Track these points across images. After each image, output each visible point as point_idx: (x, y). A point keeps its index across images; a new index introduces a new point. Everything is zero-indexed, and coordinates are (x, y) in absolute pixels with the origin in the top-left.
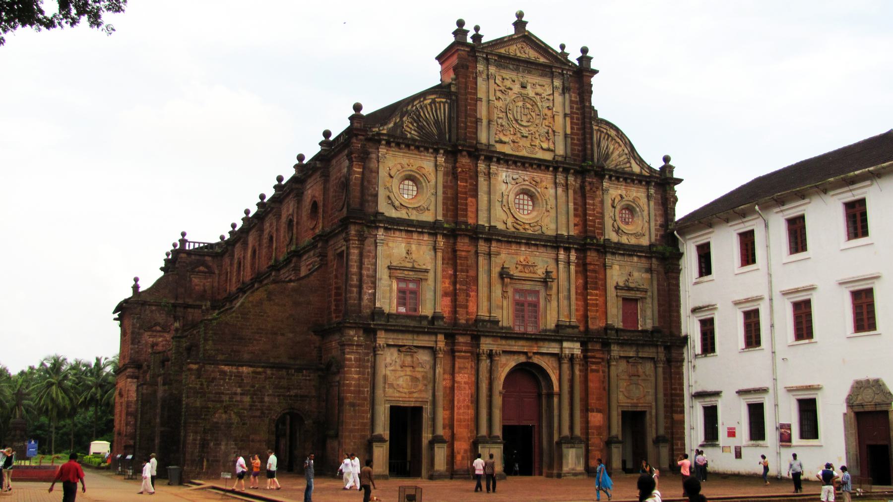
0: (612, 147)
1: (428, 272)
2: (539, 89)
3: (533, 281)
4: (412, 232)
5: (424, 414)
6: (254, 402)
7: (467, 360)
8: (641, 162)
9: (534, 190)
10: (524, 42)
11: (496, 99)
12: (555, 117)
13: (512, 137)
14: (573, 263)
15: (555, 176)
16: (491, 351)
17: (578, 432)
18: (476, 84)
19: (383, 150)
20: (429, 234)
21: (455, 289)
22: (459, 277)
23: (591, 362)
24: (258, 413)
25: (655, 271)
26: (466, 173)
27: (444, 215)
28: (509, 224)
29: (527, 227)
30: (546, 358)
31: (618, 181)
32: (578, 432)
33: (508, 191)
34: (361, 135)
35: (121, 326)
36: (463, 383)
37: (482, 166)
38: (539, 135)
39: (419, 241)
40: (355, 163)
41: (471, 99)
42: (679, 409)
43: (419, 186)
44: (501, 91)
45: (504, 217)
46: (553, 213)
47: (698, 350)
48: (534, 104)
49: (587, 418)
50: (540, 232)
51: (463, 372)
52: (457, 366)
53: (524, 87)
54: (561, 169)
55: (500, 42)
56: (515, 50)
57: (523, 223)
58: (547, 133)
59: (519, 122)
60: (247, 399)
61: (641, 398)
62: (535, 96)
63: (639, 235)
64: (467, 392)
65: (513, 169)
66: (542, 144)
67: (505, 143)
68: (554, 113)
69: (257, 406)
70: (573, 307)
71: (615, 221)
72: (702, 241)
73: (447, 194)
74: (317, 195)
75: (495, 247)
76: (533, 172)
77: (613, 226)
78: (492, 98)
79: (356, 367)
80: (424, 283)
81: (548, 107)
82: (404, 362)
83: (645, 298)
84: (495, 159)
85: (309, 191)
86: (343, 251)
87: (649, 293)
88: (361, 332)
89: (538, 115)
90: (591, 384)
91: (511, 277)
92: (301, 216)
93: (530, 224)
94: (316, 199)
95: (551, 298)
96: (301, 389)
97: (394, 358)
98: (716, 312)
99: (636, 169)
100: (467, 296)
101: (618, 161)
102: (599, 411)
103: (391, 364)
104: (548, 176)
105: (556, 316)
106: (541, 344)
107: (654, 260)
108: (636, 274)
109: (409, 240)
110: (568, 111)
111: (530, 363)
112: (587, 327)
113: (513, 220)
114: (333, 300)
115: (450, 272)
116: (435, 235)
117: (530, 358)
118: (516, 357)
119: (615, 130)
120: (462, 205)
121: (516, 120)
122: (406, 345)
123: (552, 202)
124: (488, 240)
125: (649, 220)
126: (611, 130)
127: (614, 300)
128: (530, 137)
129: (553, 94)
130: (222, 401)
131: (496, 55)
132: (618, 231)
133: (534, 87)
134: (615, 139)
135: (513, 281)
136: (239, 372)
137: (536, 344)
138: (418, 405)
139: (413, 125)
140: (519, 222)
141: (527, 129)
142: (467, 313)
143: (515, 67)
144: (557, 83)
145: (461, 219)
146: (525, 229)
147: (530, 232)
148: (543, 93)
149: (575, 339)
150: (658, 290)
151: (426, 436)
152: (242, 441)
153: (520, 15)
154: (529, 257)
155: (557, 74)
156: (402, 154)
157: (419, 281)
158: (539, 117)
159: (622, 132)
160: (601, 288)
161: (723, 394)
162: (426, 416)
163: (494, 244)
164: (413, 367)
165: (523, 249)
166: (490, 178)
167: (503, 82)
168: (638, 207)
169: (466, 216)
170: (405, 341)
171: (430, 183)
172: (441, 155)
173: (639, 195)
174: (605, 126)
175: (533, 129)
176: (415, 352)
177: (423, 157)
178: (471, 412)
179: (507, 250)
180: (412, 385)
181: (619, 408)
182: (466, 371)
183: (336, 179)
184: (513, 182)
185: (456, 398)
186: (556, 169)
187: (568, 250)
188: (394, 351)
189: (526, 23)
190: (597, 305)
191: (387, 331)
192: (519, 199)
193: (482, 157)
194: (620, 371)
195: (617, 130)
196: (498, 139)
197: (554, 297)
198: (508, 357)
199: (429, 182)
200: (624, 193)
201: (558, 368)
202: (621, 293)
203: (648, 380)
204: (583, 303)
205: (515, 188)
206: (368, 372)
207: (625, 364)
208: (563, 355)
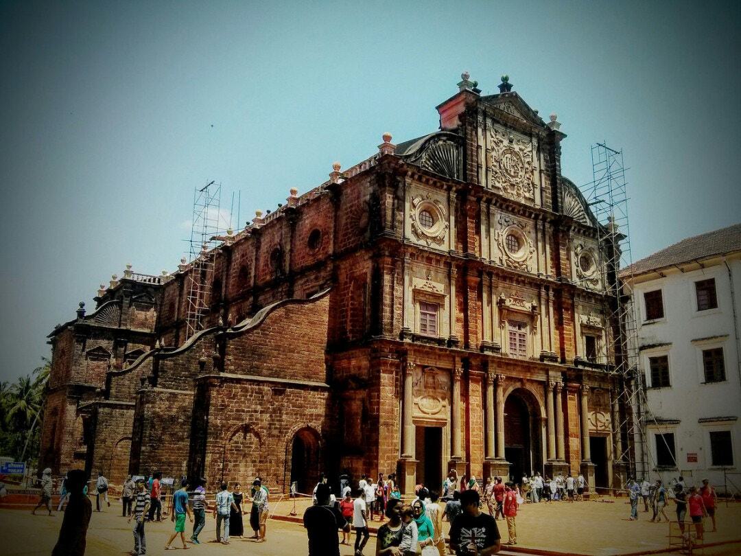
0: (573, 203)
6: (273, 420)
8: (593, 219)
9: (520, 233)
10: (510, 102)
12: (534, 171)
18: (477, 133)
19: (408, 180)
20: (446, 263)
21: (466, 316)
22: (470, 304)
32: (562, 455)
35: (54, 349)
37: (483, 206)
38: (523, 186)
40: (387, 188)
43: (435, 218)
44: (495, 142)
45: (501, 256)
47: (649, 382)
53: (511, 142)
54: (541, 217)
58: (529, 184)
60: (267, 416)
67: (499, 188)
70: (552, 340)
72: (652, 287)
74: (319, 223)
84: (494, 202)
85: (307, 222)
86: (366, 274)
91: (508, 309)
92: (295, 245)
93: (518, 263)
94: (318, 228)
96: (316, 408)
99: (589, 223)
101: (578, 215)
107: (606, 303)
110: (543, 168)
114: (348, 320)
121: (507, 170)
122: (429, 366)
124: (490, 274)
130: (243, 420)
132: (580, 277)
136: (259, 389)
137: (529, 371)
138: (438, 426)
139: (430, 162)
142: (477, 337)
144: (535, 141)
145: (470, 251)
151: (446, 458)
152: (260, 462)
153: (505, 79)
156: (422, 186)
164: (434, 388)
166: (489, 218)
167: (496, 135)
173: (593, 246)
178: (482, 435)
182: (477, 394)
183: (351, 206)
185: (471, 420)
186: (536, 218)
187: (547, 289)
188: (419, 371)
189: (511, 86)
192: (508, 239)
193: (484, 199)
195: (576, 189)
197: (539, 329)
200: (583, 244)
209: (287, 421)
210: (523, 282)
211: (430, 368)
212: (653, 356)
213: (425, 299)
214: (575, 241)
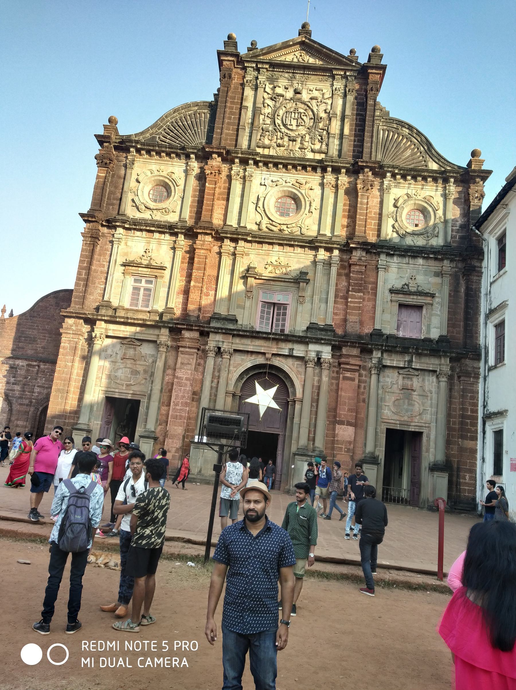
1: (165, 270)
2: (316, 94)
3: (284, 281)
4: (152, 232)
5: (140, 408)
7: (192, 357)
8: (439, 158)
12: (332, 119)
14: (335, 264)
17: (319, 443)
22: (194, 274)
24: (26, 402)
25: (446, 274)
26: (215, 175)
27: (191, 217)
29: (284, 227)
30: (290, 361)
33: (266, 192)
34: (106, 142)
36: (184, 379)
37: (236, 168)
44: (271, 99)
46: (316, 214)
49: (334, 429)
50: (299, 233)
51: (185, 368)
52: (179, 360)
53: (297, 92)
54: (329, 169)
55: (271, 50)
56: (293, 59)
57: (280, 224)
59: (289, 127)
61: (416, 416)
64: (188, 389)
66: (313, 146)
68: (331, 115)
69: (26, 395)
71: (396, 221)
76: (298, 174)
77: (393, 227)
78: (259, 105)
81: (325, 110)
82: (125, 354)
83: (432, 305)
84: (251, 162)
87: (437, 300)
89: (312, 119)
90: (342, 393)
95: (304, 300)
99: (434, 166)
102: (349, 424)
103: (111, 356)
105: (309, 319)
106: (283, 345)
109: (148, 239)
112: (345, 332)
116: (176, 234)
119: (408, 129)
120: (208, 205)
124: (235, 240)
126: (404, 129)
128: (299, 140)
129: (332, 97)
131: (266, 63)
133: (310, 92)
136: (14, 364)
137: (277, 344)
140: (274, 223)
143: (291, 75)
146: (280, 230)
147: (286, 232)
149: (323, 342)
155: (340, 77)
159: (417, 130)
161: (509, 413)
162: (142, 409)
163: (241, 243)
168: (431, 206)
172: (194, 160)
173: (432, 194)
174: (395, 126)
176: (140, 346)
180: (131, 378)
181: (383, 424)
182: (189, 367)
185: (174, 394)
186: (324, 170)
187: (329, 250)
190: (359, 307)
191: (106, 322)
195: (410, 128)
198: (242, 357)
199: (177, 186)
201: (303, 373)
202: (395, 297)
203: (427, 396)
204: (345, 307)
208: (307, 358)
209: (39, 393)
212: (496, 322)
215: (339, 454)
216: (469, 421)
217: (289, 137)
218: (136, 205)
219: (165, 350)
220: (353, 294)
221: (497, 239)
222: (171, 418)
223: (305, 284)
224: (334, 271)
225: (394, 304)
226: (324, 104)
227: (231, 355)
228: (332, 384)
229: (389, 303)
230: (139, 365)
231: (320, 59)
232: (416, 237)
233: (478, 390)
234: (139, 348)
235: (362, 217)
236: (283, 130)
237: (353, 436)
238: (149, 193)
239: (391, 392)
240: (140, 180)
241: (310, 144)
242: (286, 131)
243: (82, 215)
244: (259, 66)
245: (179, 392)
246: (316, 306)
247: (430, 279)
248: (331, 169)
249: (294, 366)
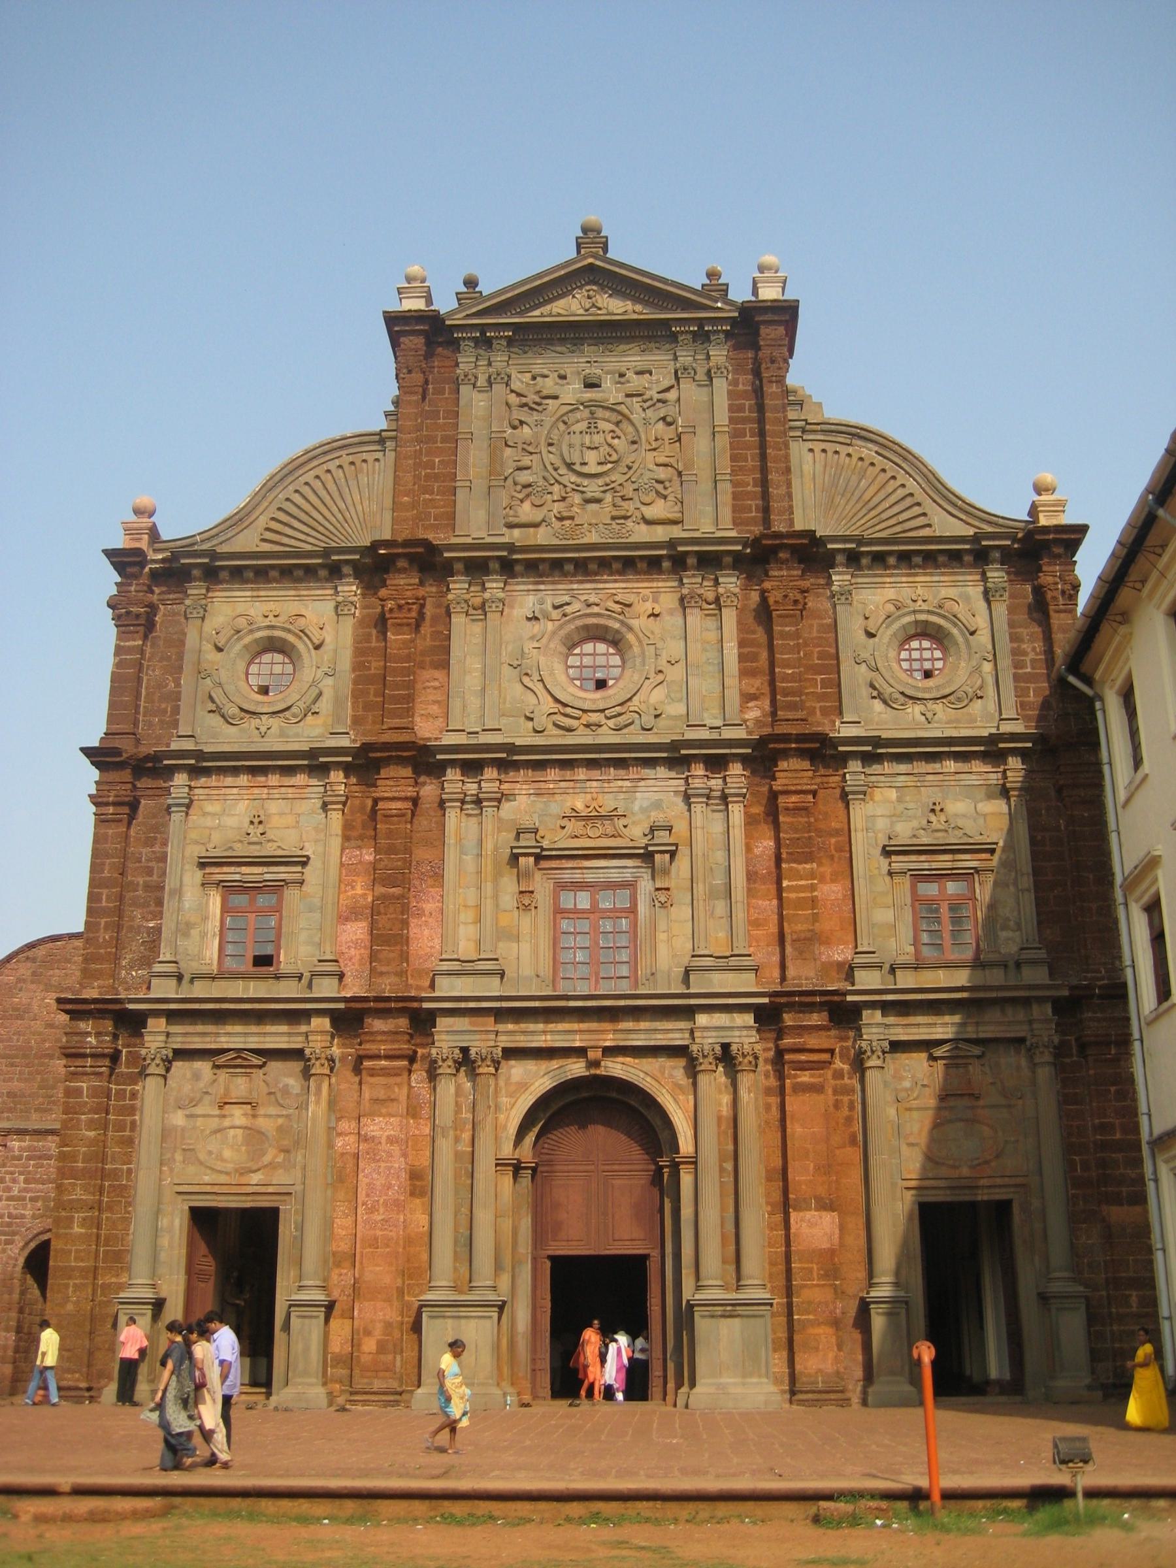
1: (304, 864)
2: (636, 382)
7: (398, 1079)
9: (617, 626)
11: (514, 428)
13: (557, 507)
15: (681, 580)
16: (465, 1050)
23: (793, 1062)
26: (410, 610)
28: (542, 721)
29: (594, 718)
31: (887, 567)
36: (383, 1141)
37: (459, 586)
39: (283, 790)
41: (445, 439)
42: (1124, 1189)
48: (622, 418)
51: (384, 1111)
52: (367, 1094)
53: (590, 385)
54: (691, 561)
57: (584, 711)
59: (577, 467)
62: (629, 399)
63: (959, 700)
64: (397, 1165)
65: (553, 583)
68: (680, 429)
70: (740, 915)
73: (370, 669)
75: (492, 780)
76: (616, 581)
79: (89, 1112)
80: (291, 894)
81: (664, 419)
88: (109, 1026)
89: (634, 442)
90: (795, 1129)
93: (602, 711)
97: (201, 1085)
98: (1160, 873)
99: (946, 525)
100: (403, 914)
102: (826, 1205)
103: (191, 1100)
104: (660, 584)
105: (689, 946)
108: (958, 807)
109: (256, 791)
111: (596, 1077)
113: (554, 707)
115: (367, 857)
116: (324, 769)
117: (596, 1064)
118: (555, 1064)
120: (397, 686)
121: (569, 466)
123: (674, 648)
124: (472, 768)
125: (995, 655)
127: (884, 883)
128: (608, 497)
133: (622, 380)
134: (872, 464)
135: (544, 864)
140: (568, 710)
141: (600, 482)
142: (405, 957)
144: (685, 358)
146: (587, 726)
148: (649, 389)
150: (1033, 841)
154: (600, 796)
156: (248, 593)
157: (277, 887)
158: (636, 446)
160: (837, 855)
162: (286, 1232)
163: (490, 773)
165: (582, 777)
168: (955, 625)
169: (409, 712)
170: (223, 1039)
171: (322, 649)
175: (617, 477)
176: (260, 1067)
177: (305, 593)
179: (536, 785)
182: (393, 1109)
184: (556, 614)
185: (363, 1181)
188: (203, 1067)
190: (814, 900)
191: (173, 1016)
194: (907, 1084)
196: (511, 519)
202: (900, 862)
205: (561, 627)
206: (133, 1123)
207: (926, 1064)
208: (694, 1048)
210: (621, 764)
211: (233, 1055)
212: (1146, 898)
213: (237, 877)
214: (861, 596)
215: (805, 1286)
216: (1119, 1156)
217: (583, 492)
218: (217, 707)
219: (328, 1072)
220: (791, 869)
221: (1119, 693)
222: (363, 1248)
223: (667, 856)
224: (736, 813)
225: (897, 879)
226: (660, 405)
227: (497, 1064)
228: (768, 1107)
229: (888, 879)
230: (266, 1116)
231: (636, 300)
232: (930, 704)
233: (1132, 1074)
234: (261, 1072)
235: (790, 672)
236: (564, 480)
237: (837, 1236)
238: (247, 674)
239: (918, 1109)
240: (220, 645)
241: (639, 505)
242: (574, 478)
243: (87, 752)
244: (488, 334)
245: (375, 1176)
246: (700, 905)
247: (980, 806)
248: (695, 561)
249: (663, 1073)
